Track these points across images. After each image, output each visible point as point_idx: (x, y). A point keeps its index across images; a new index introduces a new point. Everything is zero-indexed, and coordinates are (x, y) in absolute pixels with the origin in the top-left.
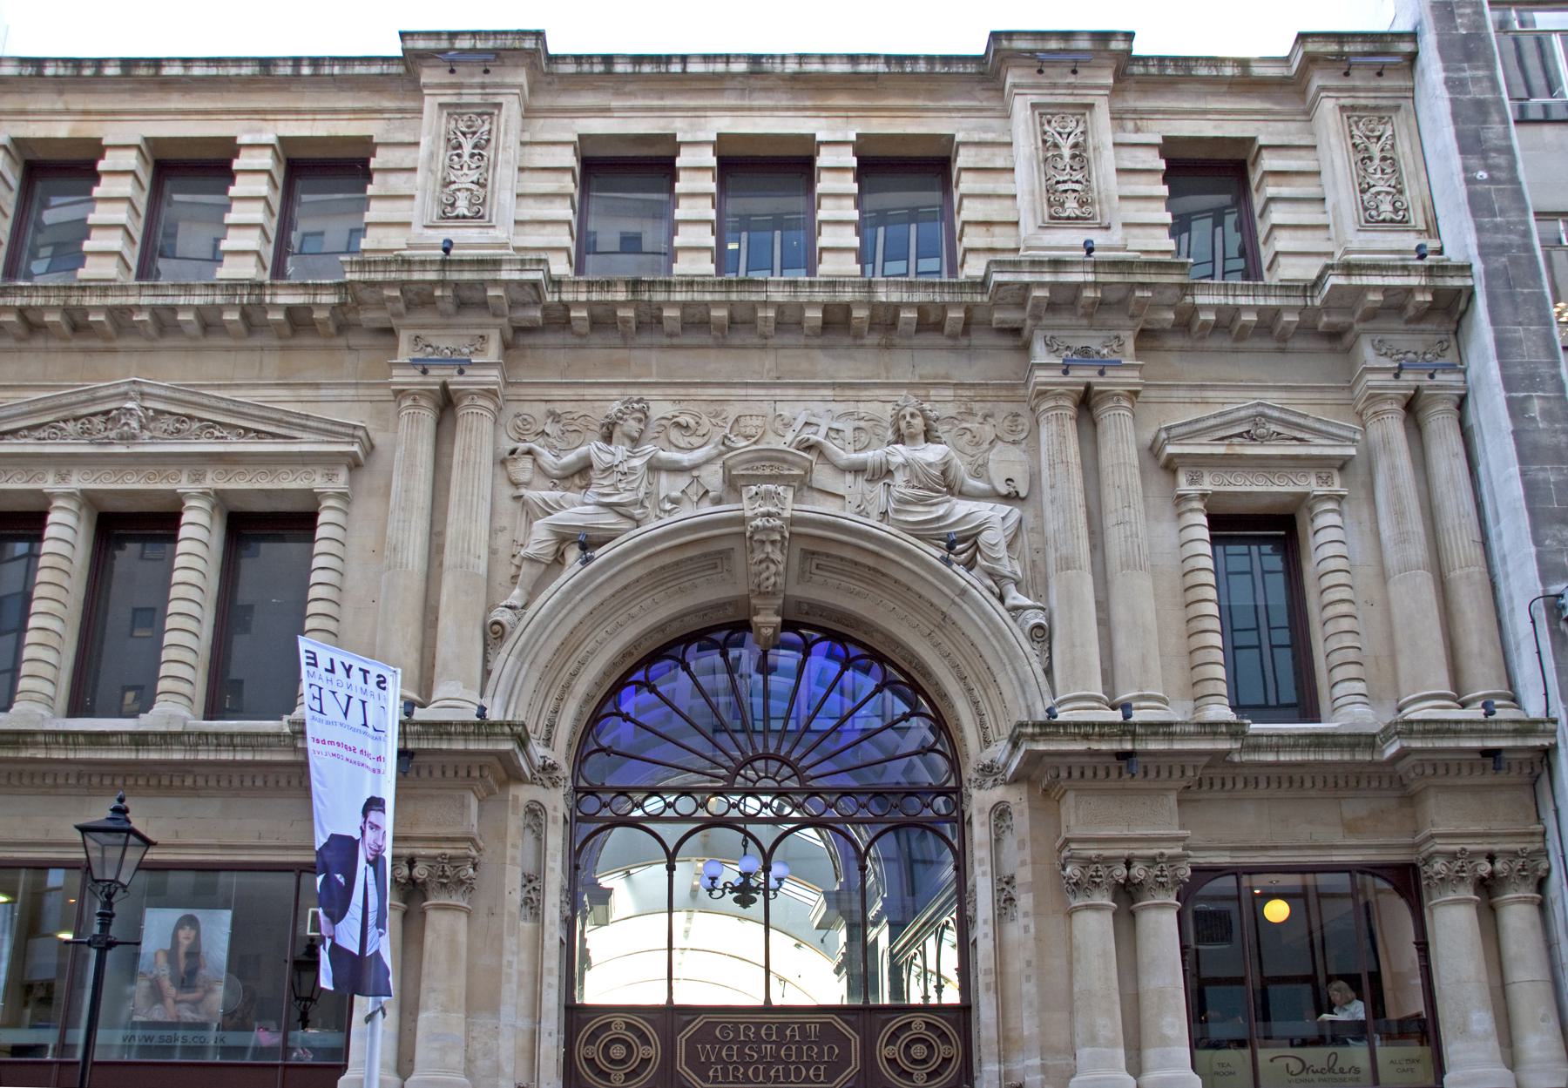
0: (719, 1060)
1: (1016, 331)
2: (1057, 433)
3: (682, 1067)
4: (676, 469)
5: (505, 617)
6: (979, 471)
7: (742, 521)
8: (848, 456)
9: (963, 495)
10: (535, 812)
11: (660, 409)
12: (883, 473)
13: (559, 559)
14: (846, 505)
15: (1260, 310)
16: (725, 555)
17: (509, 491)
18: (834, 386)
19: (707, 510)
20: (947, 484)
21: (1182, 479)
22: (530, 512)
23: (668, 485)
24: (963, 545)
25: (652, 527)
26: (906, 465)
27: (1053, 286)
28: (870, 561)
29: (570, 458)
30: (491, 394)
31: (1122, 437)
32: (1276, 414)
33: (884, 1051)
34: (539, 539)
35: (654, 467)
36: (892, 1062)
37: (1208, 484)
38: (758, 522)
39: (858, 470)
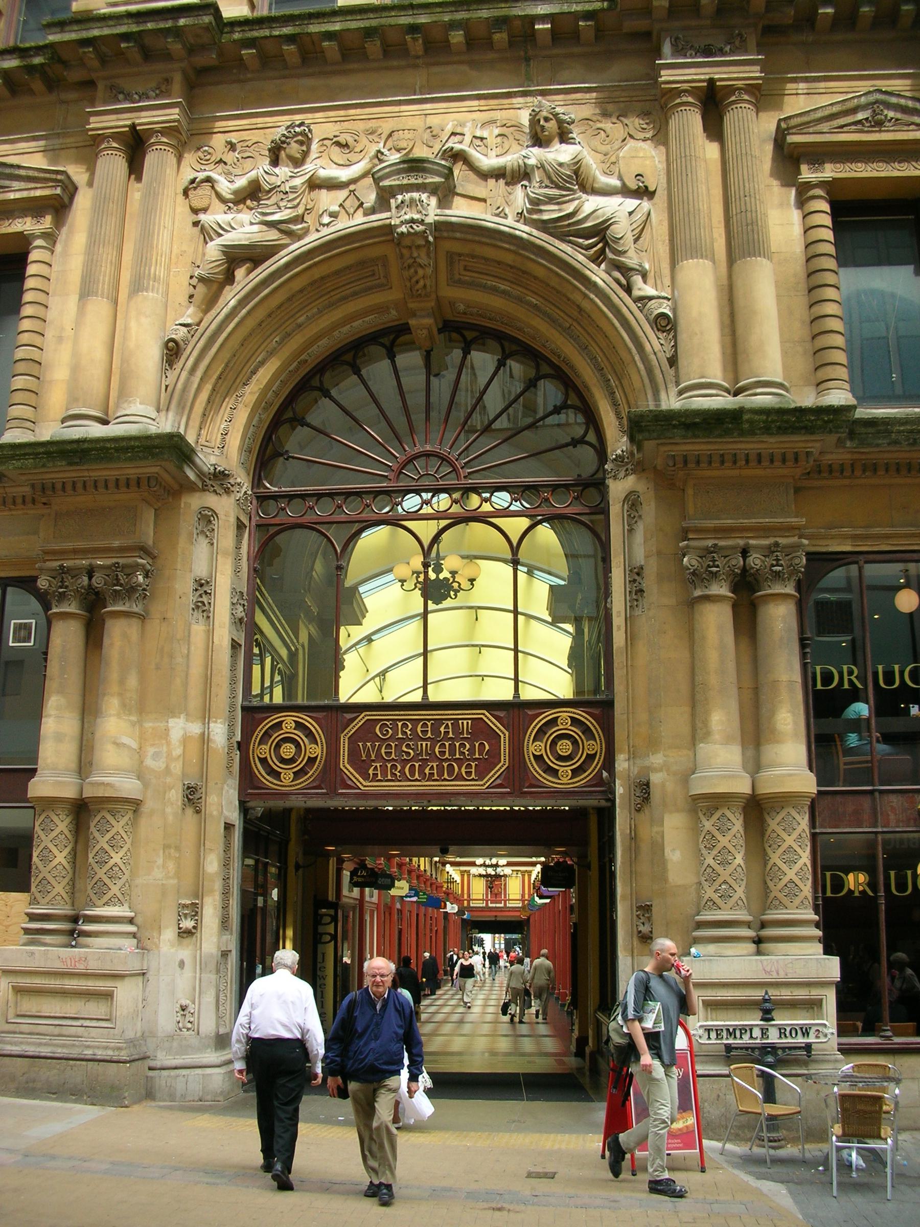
3: (344, 763)
4: (332, 185)
8: (487, 161)
9: (595, 192)
10: (207, 518)
12: (520, 175)
13: (229, 278)
19: (359, 221)
23: (328, 200)
25: (311, 240)
29: (241, 182)
35: (314, 184)
37: (829, 172)
38: (403, 229)
39: (499, 174)
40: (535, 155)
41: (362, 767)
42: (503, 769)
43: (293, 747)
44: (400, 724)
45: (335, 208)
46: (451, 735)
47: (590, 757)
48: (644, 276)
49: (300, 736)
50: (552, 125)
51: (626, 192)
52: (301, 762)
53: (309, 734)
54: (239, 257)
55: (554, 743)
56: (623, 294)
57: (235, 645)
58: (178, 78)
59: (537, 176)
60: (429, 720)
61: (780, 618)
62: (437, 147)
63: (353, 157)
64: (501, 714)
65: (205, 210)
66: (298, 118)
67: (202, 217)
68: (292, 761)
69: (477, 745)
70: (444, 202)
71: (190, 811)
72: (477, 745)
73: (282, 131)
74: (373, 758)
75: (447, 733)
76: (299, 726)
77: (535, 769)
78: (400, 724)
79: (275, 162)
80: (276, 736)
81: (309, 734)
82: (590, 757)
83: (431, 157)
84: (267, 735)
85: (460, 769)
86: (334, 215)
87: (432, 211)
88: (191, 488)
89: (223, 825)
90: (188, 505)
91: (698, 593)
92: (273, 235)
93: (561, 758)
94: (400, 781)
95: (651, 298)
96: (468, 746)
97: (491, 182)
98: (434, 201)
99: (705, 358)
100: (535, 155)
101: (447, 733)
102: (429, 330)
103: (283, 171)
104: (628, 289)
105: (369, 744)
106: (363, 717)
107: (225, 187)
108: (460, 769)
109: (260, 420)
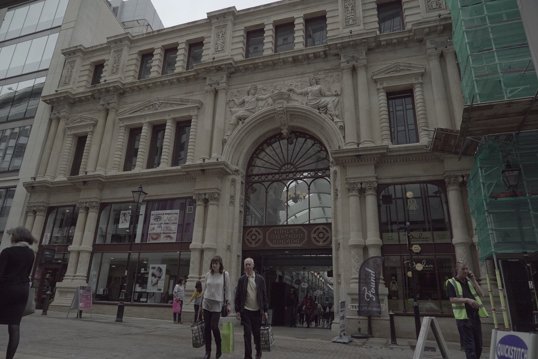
0: (275, 238)
1: (338, 55)
2: (347, 78)
3: (268, 241)
4: (262, 100)
5: (225, 137)
6: (329, 90)
7: (275, 109)
8: (299, 91)
9: (325, 96)
10: (233, 181)
11: (259, 87)
12: (306, 94)
13: (238, 123)
14: (298, 102)
15: (397, 39)
16: (273, 117)
17: (228, 110)
18: (297, 75)
19: (269, 108)
20: (321, 94)
21: (378, 85)
22: (232, 113)
23: (261, 103)
24: (324, 108)
25: (257, 113)
26: (311, 91)
27: (342, 43)
28: (304, 115)
29: (240, 100)
30: (224, 89)
31: (362, 76)
32: (402, 64)
33: (313, 235)
34: (233, 119)
35: (258, 100)
36: (315, 238)
37: (385, 85)
38: (278, 109)
39: (301, 94)
40: (310, 89)
45: (263, 105)
48: (337, 116)
49: (257, 234)
50: (314, 81)
51: (332, 95)
52: (257, 240)
54: (240, 119)
55: (318, 234)
56: (331, 121)
57: (241, 212)
58: (225, 76)
59: (310, 94)
61: (371, 201)
62: (287, 88)
63: (267, 92)
65: (233, 108)
66: (254, 83)
67: (232, 109)
68: (255, 240)
70: (288, 103)
71: (228, 252)
73: (249, 87)
77: (313, 240)
79: (248, 95)
80: (251, 234)
81: (259, 233)
83: (285, 91)
86: (262, 107)
87: (286, 104)
88: (229, 174)
89: (236, 256)
90: (229, 178)
91: (350, 194)
92: (247, 113)
93: (320, 238)
95: (338, 122)
97: (300, 96)
98: (285, 102)
99: (351, 137)
100: (310, 89)
102: (287, 133)
103: (250, 97)
104: (333, 120)
106: (271, 229)
107: (237, 101)
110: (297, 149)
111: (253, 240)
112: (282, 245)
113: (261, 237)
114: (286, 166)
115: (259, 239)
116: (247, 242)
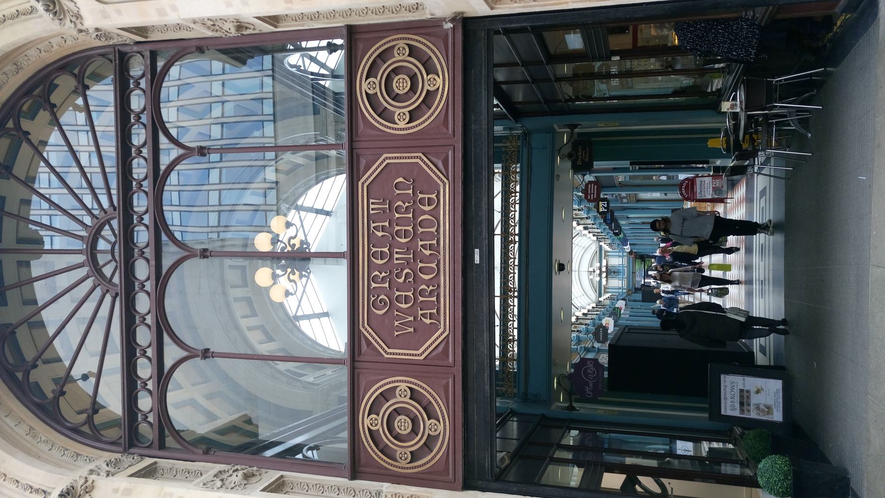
3: (420, 354)
36: (413, 116)
41: (422, 333)
42: (425, 159)
43: (399, 418)
44: (374, 285)
46: (387, 224)
47: (413, 52)
49: (387, 408)
52: (415, 408)
53: (385, 396)
60: (369, 250)
64: (363, 162)
68: (414, 421)
69: (398, 192)
72: (398, 192)
74: (411, 318)
75: (383, 229)
76: (374, 409)
78: (374, 285)
80: (386, 439)
81: (385, 396)
82: (413, 52)
84: (385, 451)
85: (424, 213)
93: (413, 89)
94: (439, 286)
96: (400, 203)
101: (383, 229)
105: (396, 323)
106: (366, 331)
108: (424, 213)
109: (46, 442)
110: (61, 221)
111: (415, 431)
112: (445, 280)
113: (402, 384)
114: (101, 259)
115: (414, 395)
116: (426, 462)
